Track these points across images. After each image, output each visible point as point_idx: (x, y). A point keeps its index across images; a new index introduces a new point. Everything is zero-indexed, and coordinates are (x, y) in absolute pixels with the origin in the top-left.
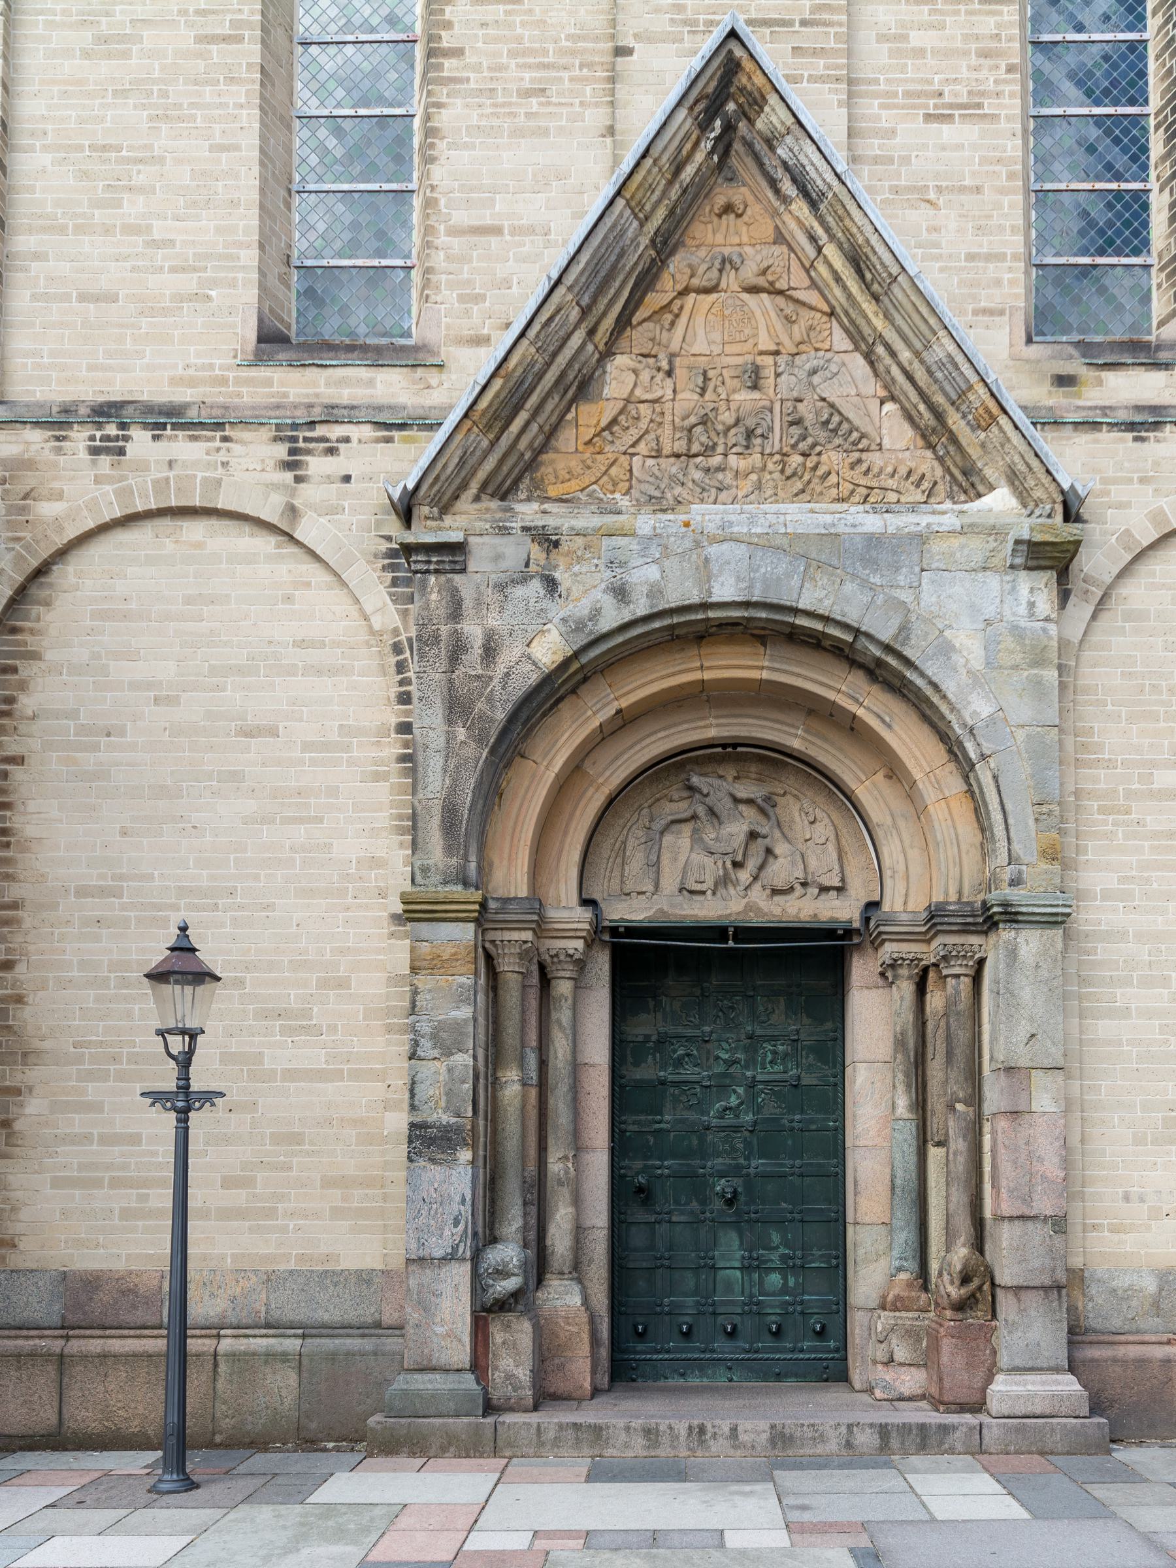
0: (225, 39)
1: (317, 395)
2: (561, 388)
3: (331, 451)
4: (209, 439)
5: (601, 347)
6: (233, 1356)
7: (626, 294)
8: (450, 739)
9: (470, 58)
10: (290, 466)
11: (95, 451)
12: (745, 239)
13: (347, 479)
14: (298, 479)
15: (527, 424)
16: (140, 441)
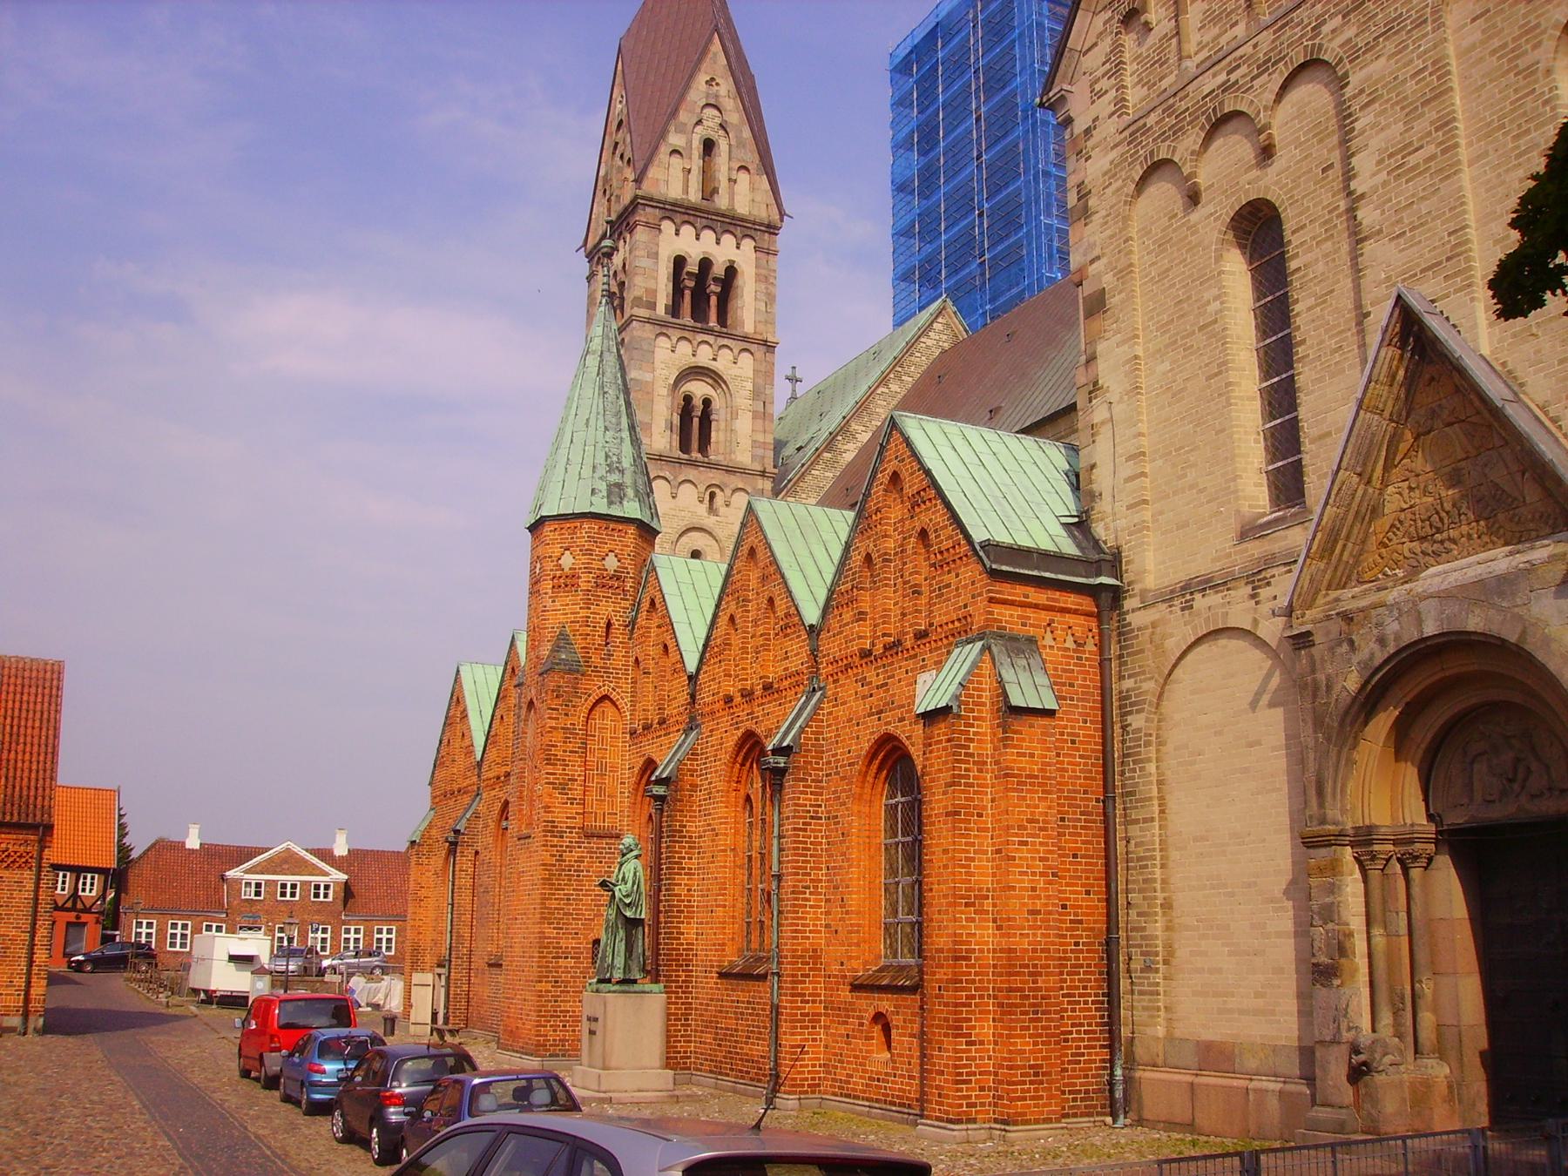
0: (1216, 375)
1: (1265, 551)
2: (1360, 519)
3: (1268, 584)
4: (1222, 591)
5: (1378, 486)
6: (1255, 1090)
7: (1384, 453)
8: (1316, 740)
9: (1308, 343)
10: (1253, 596)
11: (1183, 609)
12: (1442, 395)
13: (1275, 598)
14: (1257, 603)
15: (1345, 546)
16: (1199, 602)
